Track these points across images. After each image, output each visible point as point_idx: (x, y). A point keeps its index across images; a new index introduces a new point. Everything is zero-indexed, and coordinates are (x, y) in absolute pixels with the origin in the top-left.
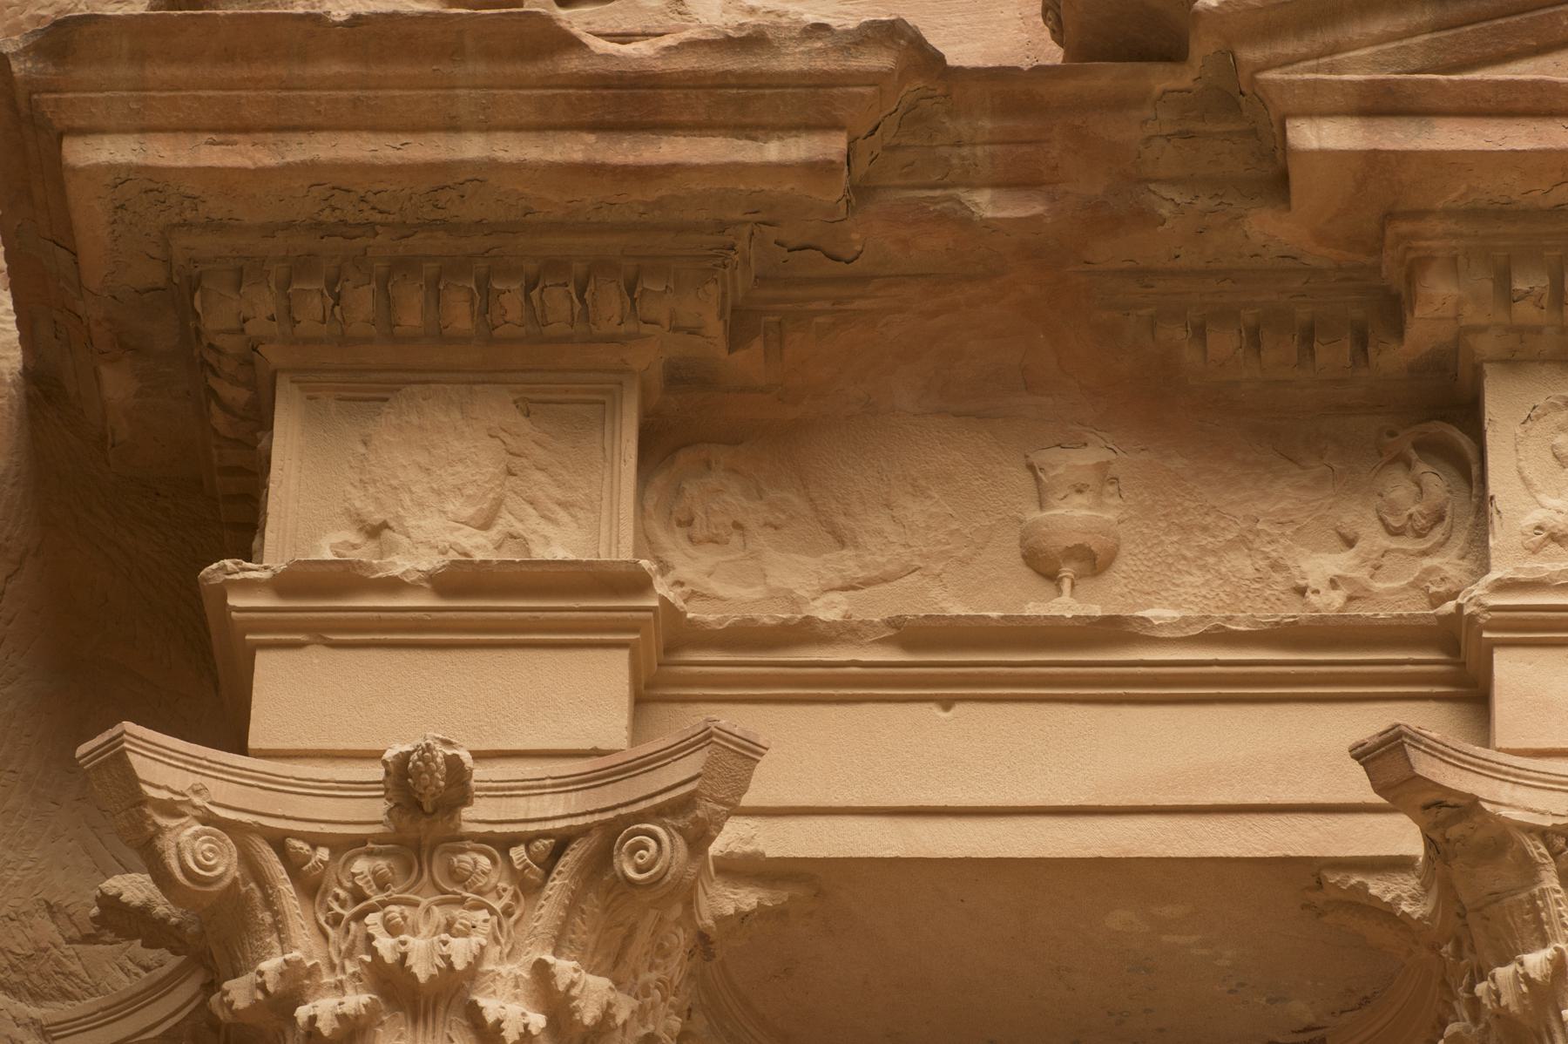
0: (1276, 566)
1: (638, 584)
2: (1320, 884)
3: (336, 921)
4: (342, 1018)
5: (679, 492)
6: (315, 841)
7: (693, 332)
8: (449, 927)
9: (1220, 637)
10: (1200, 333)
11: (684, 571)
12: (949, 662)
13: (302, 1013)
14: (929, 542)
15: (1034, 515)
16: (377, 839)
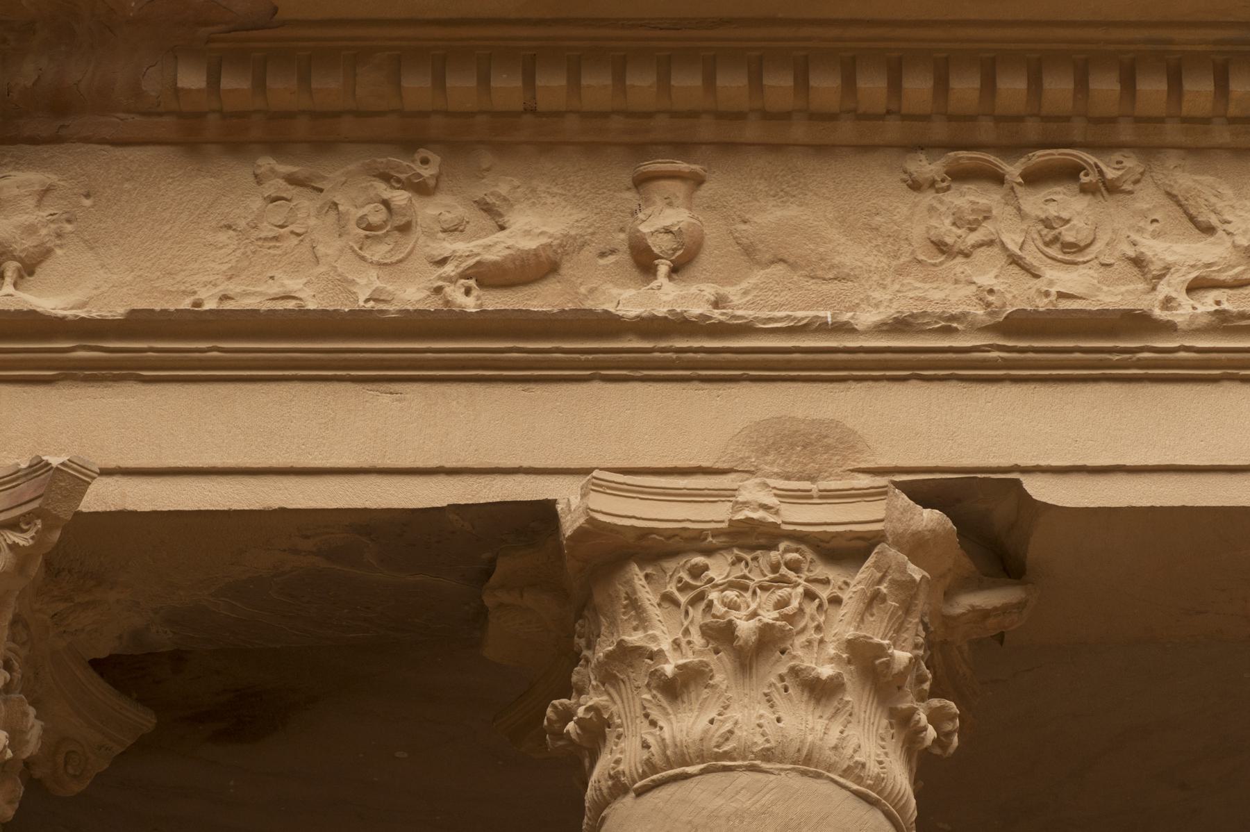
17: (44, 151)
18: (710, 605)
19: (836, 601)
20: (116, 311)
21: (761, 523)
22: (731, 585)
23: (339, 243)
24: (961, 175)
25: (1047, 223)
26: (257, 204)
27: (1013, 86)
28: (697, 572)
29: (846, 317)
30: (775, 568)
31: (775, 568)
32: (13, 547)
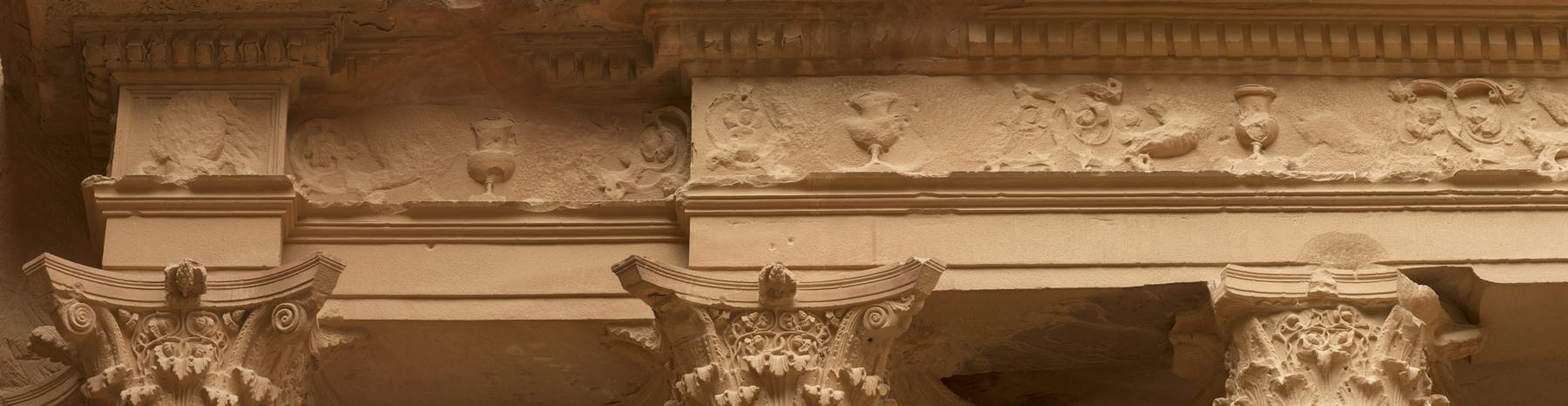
0: (590, 177)
1: (287, 186)
2: (607, 333)
3: (141, 349)
4: (142, 396)
5: (306, 142)
6: (132, 310)
7: (314, 65)
8: (193, 353)
9: (563, 212)
10: (555, 63)
11: (308, 180)
12: (433, 224)
13: (124, 394)
14: (425, 166)
15: (474, 152)
16: (160, 309)
17: (889, 79)
18: (1301, 342)
19: (1373, 339)
20: (942, 171)
21: (1326, 294)
22: (1313, 330)
23: (1067, 133)
24: (1422, 93)
25: (1473, 120)
26: (1017, 110)
27: (1446, 42)
28: (1292, 323)
29: (1364, 175)
30: (1337, 320)
31: (1337, 320)
32: (897, 311)
